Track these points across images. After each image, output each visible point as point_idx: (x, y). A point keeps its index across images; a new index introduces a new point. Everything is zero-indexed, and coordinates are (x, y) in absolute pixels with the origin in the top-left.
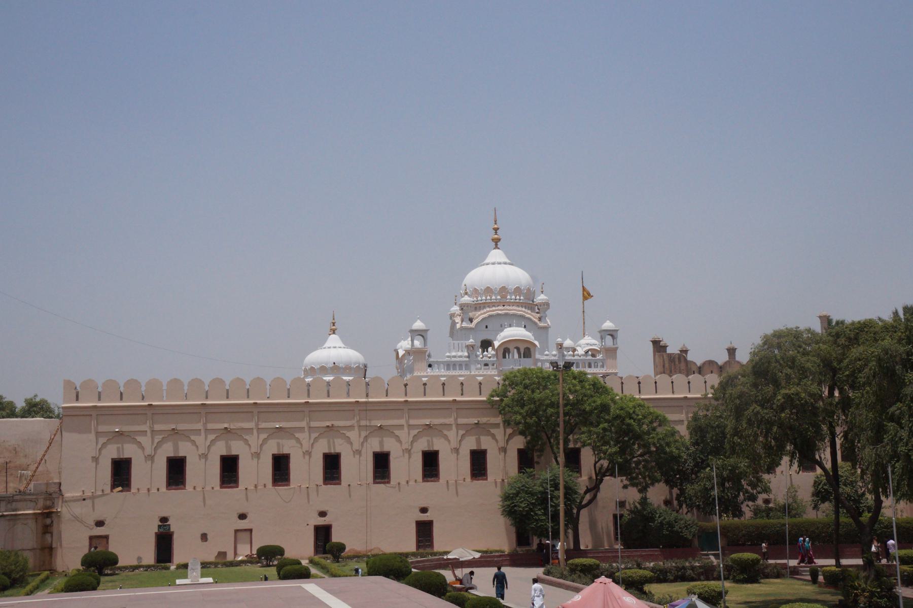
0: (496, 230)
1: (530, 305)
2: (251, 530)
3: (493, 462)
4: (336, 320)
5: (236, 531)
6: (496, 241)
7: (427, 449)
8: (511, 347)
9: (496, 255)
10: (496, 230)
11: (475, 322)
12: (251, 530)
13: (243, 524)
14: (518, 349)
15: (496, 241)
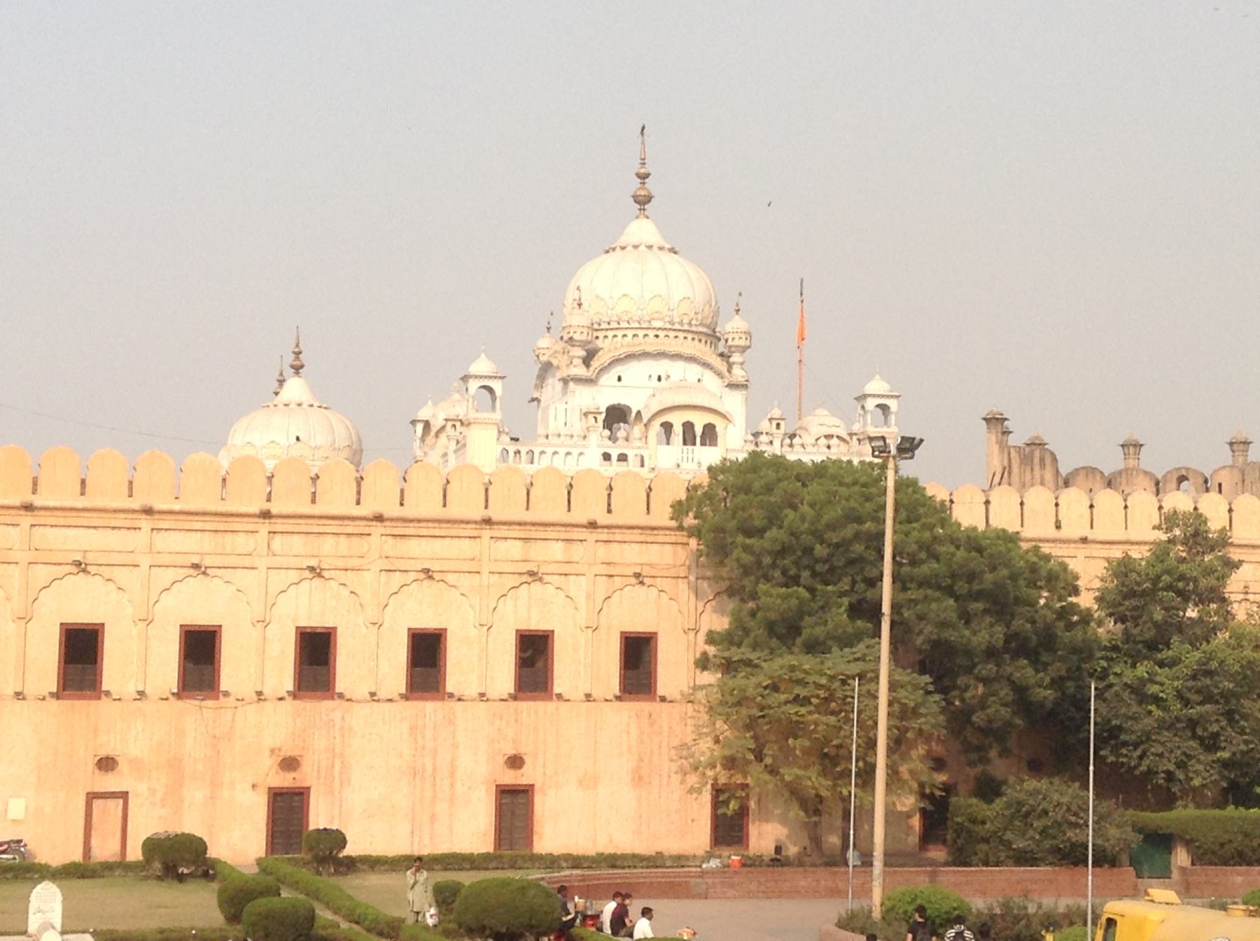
0: (643, 177)
1: (712, 337)
2: (124, 795)
3: (674, 668)
4: (302, 347)
5: (92, 797)
6: (643, 201)
7: (525, 628)
8: (677, 420)
9: (642, 230)
10: (643, 177)
11: (596, 364)
12: (124, 795)
13: (111, 783)
14: (688, 427)
15: (643, 201)
